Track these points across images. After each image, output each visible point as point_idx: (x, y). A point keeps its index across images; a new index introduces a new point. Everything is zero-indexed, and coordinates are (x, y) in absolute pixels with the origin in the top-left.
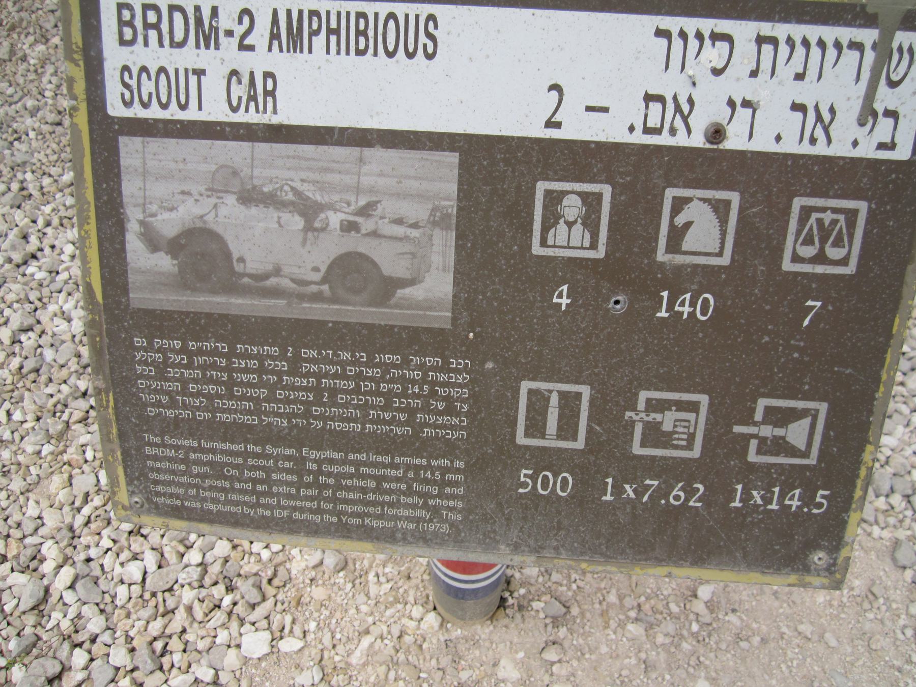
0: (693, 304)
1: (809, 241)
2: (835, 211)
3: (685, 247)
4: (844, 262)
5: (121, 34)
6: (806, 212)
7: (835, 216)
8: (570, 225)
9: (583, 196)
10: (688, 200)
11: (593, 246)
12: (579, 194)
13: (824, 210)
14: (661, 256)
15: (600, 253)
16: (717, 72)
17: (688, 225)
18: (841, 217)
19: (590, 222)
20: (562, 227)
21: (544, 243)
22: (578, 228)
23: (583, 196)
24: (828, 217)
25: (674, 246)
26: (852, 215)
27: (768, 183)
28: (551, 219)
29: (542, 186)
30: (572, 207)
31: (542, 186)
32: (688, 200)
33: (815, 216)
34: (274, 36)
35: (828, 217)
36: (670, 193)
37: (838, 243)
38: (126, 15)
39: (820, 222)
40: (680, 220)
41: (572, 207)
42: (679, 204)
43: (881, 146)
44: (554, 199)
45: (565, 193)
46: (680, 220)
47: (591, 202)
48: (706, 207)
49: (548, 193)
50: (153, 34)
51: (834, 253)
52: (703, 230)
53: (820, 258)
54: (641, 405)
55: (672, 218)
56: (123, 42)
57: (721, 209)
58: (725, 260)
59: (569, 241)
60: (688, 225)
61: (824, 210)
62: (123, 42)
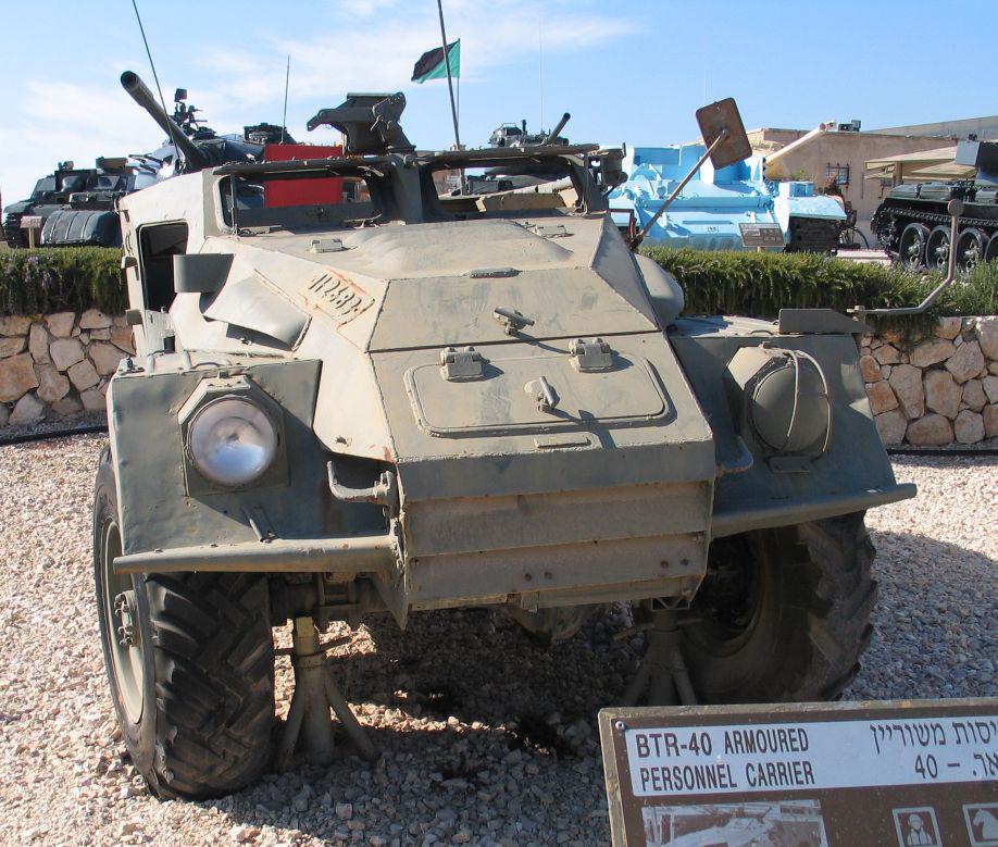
3: (985, 835)
5: (640, 751)
8: (918, 832)
10: (977, 810)
12: (919, 814)
17: (981, 825)
19: (928, 828)
20: (914, 834)
22: (923, 833)
28: (906, 830)
31: (895, 812)
32: (977, 810)
34: (728, 745)
38: (642, 741)
42: (973, 813)
44: (904, 818)
45: (910, 814)
46: (976, 822)
47: (925, 817)
48: (987, 813)
49: (900, 816)
55: (972, 820)
56: (641, 755)
60: (981, 825)
62: (641, 755)
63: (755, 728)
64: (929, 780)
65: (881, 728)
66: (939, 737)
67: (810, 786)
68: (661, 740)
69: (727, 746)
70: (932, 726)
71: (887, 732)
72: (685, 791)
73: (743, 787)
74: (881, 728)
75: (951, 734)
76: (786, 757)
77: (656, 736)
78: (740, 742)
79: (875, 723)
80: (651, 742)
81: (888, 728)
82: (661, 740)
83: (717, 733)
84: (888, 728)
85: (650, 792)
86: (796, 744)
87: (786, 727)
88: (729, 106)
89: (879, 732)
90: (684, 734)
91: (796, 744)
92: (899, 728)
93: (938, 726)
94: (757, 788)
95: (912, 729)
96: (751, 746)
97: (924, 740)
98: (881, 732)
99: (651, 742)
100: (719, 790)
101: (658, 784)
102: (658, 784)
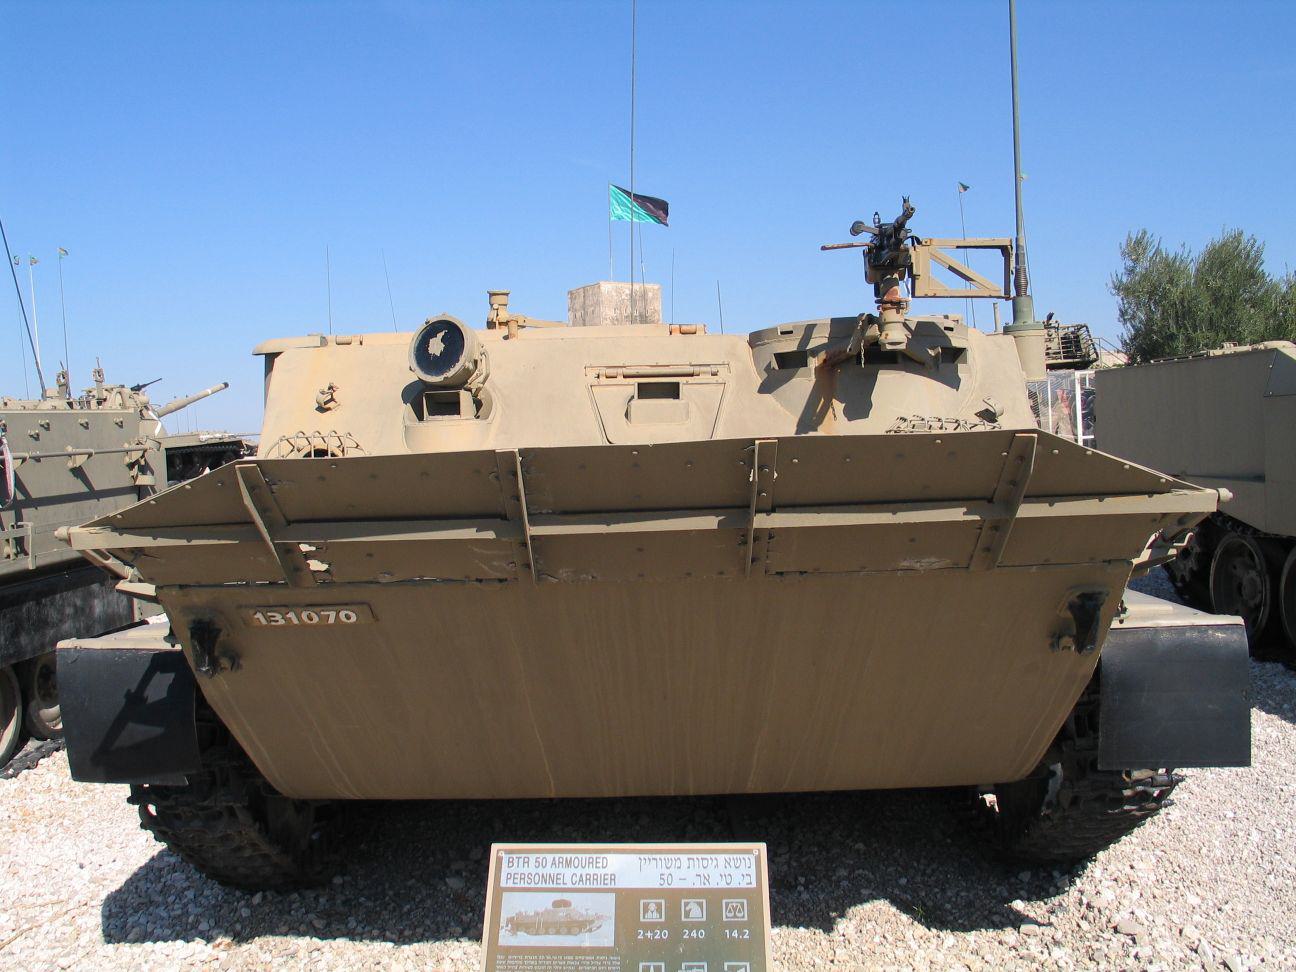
0: (697, 933)
1: (730, 911)
4: (743, 917)
6: (727, 904)
9: (655, 903)
10: (688, 903)
11: (661, 917)
14: (683, 919)
15: (663, 919)
17: (690, 910)
21: (644, 917)
23: (655, 903)
25: (687, 916)
26: (742, 904)
27: (713, 898)
28: (646, 910)
29: (642, 902)
30: (652, 907)
32: (688, 903)
36: (683, 901)
37: (740, 911)
40: (687, 908)
41: (652, 907)
42: (686, 904)
43: (748, 884)
45: (649, 904)
46: (687, 908)
47: (659, 906)
51: (741, 915)
52: (696, 912)
53: (735, 916)
54: (683, 967)
57: (700, 905)
58: (704, 919)
59: (652, 916)
60: (690, 910)
64: (666, 886)
66: (678, 864)
67: (613, 886)
68: (521, 860)
71: (647, 861)
72: (533, 885)
73: (570, 885)
76: (591, 871)
77: (519, 858)
79: (642, 856)
80: (516, 860)
81: (650, 860)
82: (521, 860)
85: (510, 884)
86: (600, 865)
87: (594, 856)
88: (676, 396)
89: (643, 861)
90: (533, 857)
91: (600, 865)
93: (679, 859)
94: (577, 886)
99: (516, 860)
100: (555, 886)
101: (516, 881)
102: (516, 881)
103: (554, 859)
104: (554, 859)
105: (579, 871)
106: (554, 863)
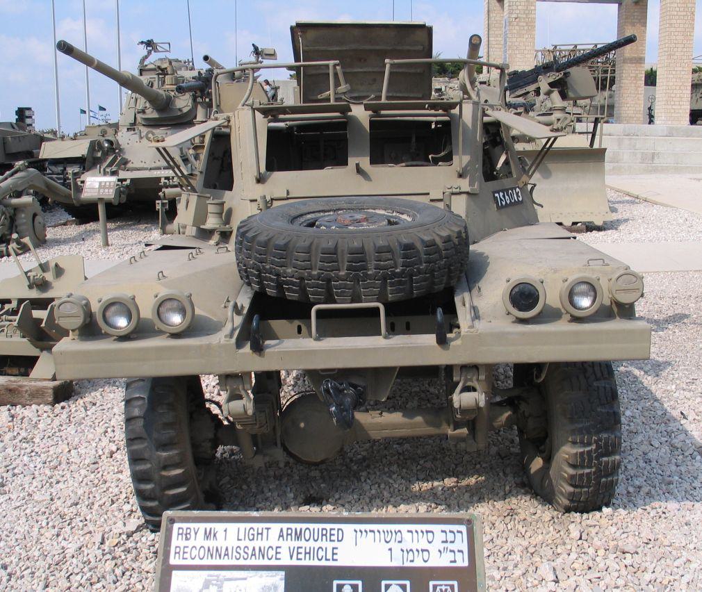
2: (446, 585)
6: (435, 587)
7: (446, 587)
13: (441, 585)
16: (400, 542)
18: (449, 587)
24: (444, 588)
26: (452, 587)
33: (438, 588)
35: (444, 588)
39: (441, 590)
50: (260, 536)
61: (441, 585)
63: (304, 526)
65: (361, 531)
69: (280, 536)
70: (395, 531)
71: (364, 533)
74: (361, 531)
75: (440, 537)
78: (291, 535)
81: (366, 531)
83: (276, 528)
84: (366, 531)
89: (359, 533)
92: (373, 531)
95: (382, 532)
96: (298, 536)
97: (388, 540)
98: (378, 534)
103: (282, 530)
104: (282, 530)
105: (311, 544)
106: (281, 536)
